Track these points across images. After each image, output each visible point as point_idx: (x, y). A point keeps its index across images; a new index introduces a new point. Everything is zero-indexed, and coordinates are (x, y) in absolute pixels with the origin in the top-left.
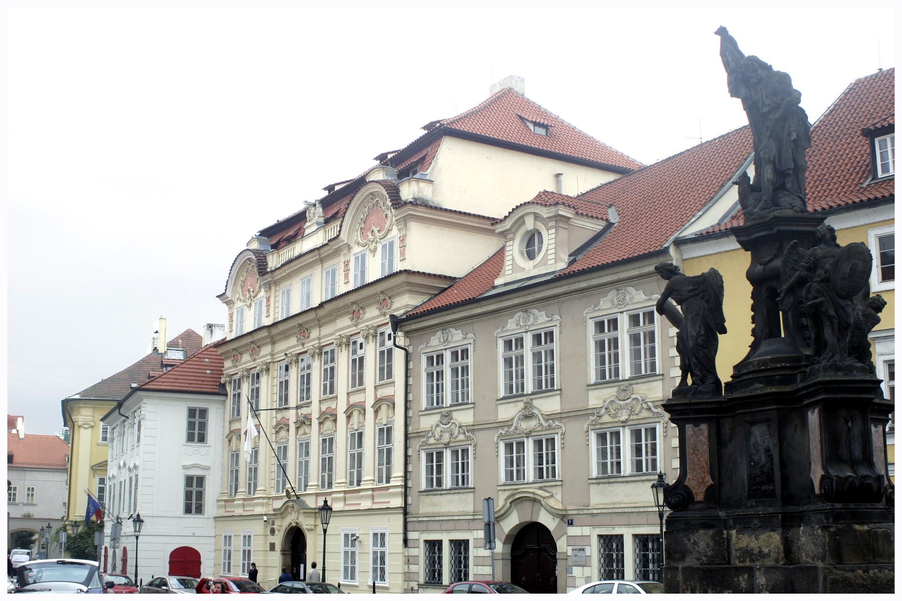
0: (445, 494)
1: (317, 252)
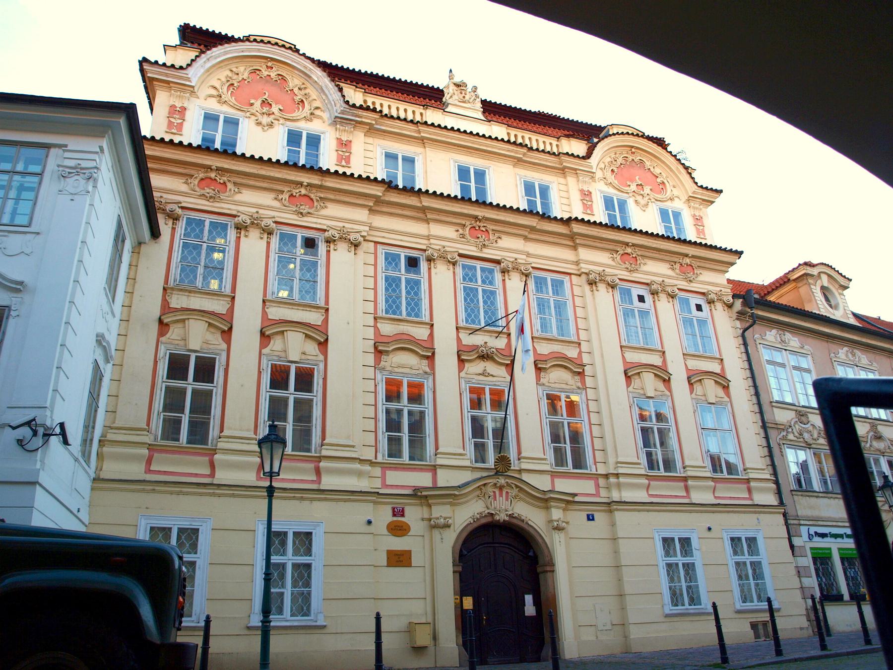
0: (822, 497)
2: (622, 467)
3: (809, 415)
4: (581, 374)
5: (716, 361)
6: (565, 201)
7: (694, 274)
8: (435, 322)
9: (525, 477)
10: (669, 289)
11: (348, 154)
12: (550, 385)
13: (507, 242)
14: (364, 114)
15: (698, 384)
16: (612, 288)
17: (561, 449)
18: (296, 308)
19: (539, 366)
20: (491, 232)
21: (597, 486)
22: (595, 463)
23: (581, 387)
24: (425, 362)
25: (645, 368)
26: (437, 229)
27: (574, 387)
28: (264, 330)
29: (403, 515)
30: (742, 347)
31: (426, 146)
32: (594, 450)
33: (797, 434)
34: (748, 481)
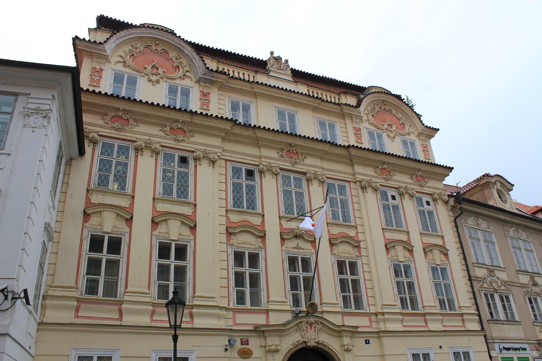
0: (506, 324)
1: (319, 101)
2: (386, 308)
3: (495, 271)
4: (358, 247)
5: (440, 237)
6: (344, 134)
7: (424, 181)
8: (265, 213)
9: (325, 316)
10: (410, 192)
11: (208, 102)
12: (339, 254)
13: (309, 161)
14: (218, 76)
15: (430, 252)
16: (375, 190)
17: (347, 296)
18: (175, 203)
19: (332, 242)
20: (299, 154)
21: (371, 321)
22: (369, 305)
23: (358, 255)
24: (260, 240)
25: (398, 243)
26: (265, 152)
27: (354, 256)
28: (154, 219)
29: (248, 344)
30: (455, 228)
31: (257, 97)
32: (368, 297)
33: (489, 284)
34: (462, 315)
